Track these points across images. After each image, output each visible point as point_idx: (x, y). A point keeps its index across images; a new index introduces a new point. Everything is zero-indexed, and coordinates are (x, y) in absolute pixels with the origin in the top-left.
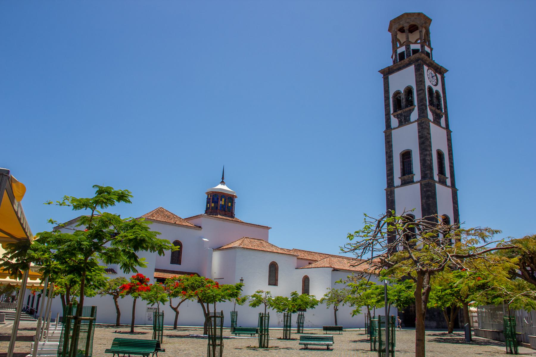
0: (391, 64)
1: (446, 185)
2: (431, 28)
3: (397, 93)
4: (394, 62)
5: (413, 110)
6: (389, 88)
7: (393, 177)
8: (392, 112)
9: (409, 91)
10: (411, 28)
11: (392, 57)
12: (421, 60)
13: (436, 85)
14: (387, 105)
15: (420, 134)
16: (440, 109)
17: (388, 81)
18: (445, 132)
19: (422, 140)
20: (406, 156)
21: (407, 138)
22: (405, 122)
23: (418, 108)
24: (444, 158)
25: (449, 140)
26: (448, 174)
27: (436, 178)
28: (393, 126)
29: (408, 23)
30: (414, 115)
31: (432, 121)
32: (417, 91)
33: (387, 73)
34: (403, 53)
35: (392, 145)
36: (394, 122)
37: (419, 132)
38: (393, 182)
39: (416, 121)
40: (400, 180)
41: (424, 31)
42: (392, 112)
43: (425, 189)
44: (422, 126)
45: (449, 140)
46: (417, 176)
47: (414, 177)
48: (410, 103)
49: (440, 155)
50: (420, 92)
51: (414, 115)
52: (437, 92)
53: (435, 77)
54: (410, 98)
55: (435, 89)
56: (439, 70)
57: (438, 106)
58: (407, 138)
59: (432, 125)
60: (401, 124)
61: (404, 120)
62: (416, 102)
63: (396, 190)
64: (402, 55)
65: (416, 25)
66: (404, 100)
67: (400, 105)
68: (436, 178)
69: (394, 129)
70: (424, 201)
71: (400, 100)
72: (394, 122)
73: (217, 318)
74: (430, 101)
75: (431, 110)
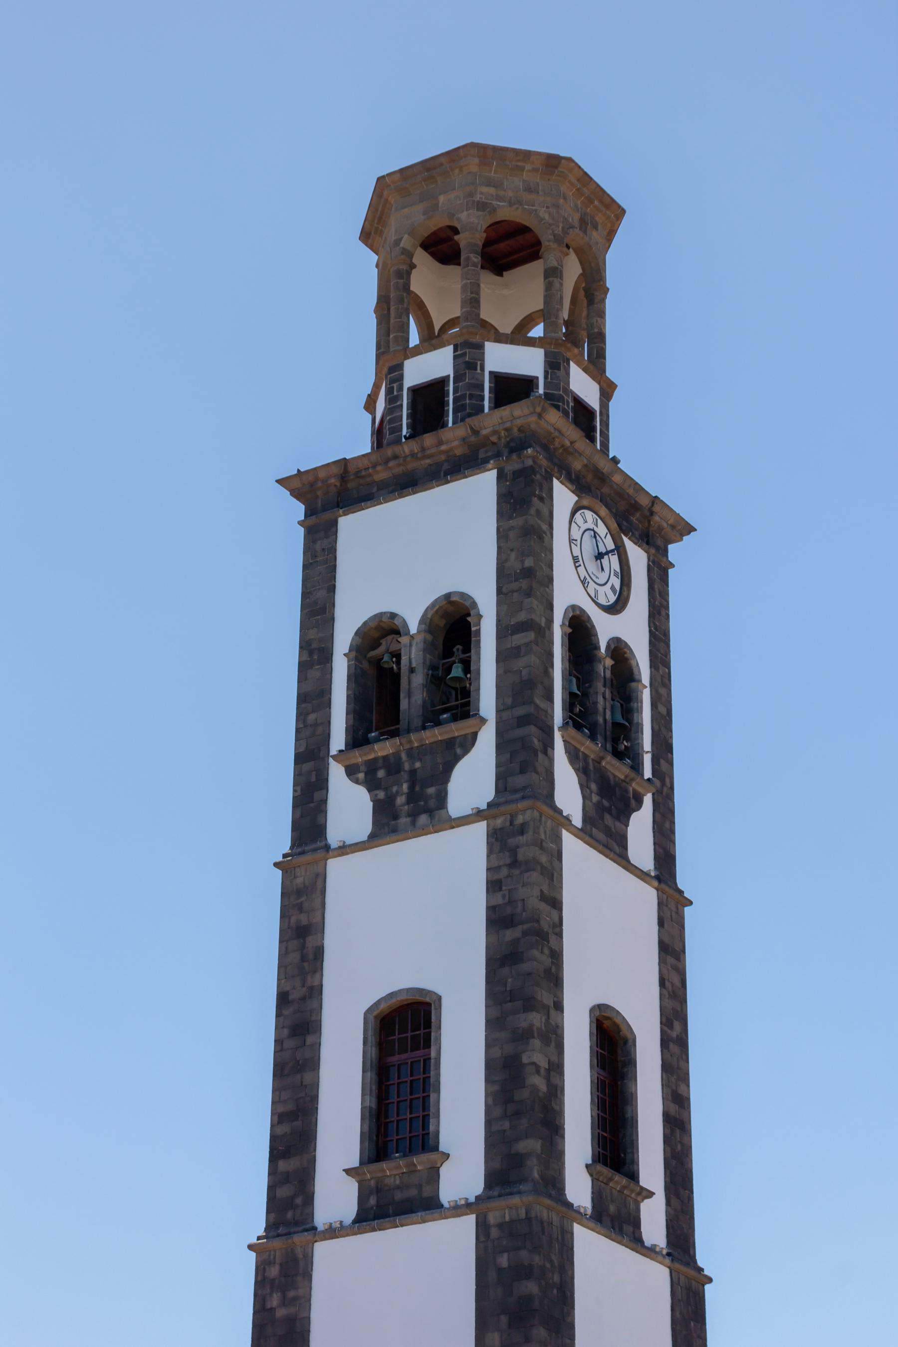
0: (357, 443)
1: (636, 1242)
2: (619, 263)
3: (382, 631)
4: (378, 434)
5: (468, 742)
6: (332, 589)
7: (313, 1161)
8: (338, 740)
9: (453, 625)
10: (493, 248)
11: (370, 405)
12: (536, 443)
13: (616, 608)
14: (312, 701)
15: (498, 899)
16: (632, 756)
17: (332, 551)
18: (647, 896)
19: (510, 935)
20: (404, 1030)
21: (413, 915)
22: (414, 815)
23: (499, 733)
24: (631, 1062)
25: (671, 951)
26: (651, 1168)
27: (579, 1188)
28: (335, 834)
29: (482, 206)
30: (473, 780)
31: (577, 821)
32: (503, 632)
33: (329, 497)
34: (439, 384)
35: (319, 953)
37: (493, 886)
38: (309, 1199)
39: (479, 815)
41: (572, 270)
42: (338, 740)
43: (504, 1261)
44: (514, 851)
45: (671, 951)
46: (463, 1170)
47: (446, 1172)
48: (454, 699)
49: (611, 1043)
50: (518, 639)
51: (473, 780)
52: (619, 651)
53: (614, 559)
54: (457, 671)
55: (606, 628)
56: (642, 522)
57: (620, 737)
58: (413, 915)
59: (570, 844)
60: (388, 824)
64: (429, 398)
65: (524, 230)
66: (419, 679)
67: (391, 708)
68: (579, 1188)
69: (345, 849)
71: (396, 677)
74: (571, 701)
75: (574, 756)
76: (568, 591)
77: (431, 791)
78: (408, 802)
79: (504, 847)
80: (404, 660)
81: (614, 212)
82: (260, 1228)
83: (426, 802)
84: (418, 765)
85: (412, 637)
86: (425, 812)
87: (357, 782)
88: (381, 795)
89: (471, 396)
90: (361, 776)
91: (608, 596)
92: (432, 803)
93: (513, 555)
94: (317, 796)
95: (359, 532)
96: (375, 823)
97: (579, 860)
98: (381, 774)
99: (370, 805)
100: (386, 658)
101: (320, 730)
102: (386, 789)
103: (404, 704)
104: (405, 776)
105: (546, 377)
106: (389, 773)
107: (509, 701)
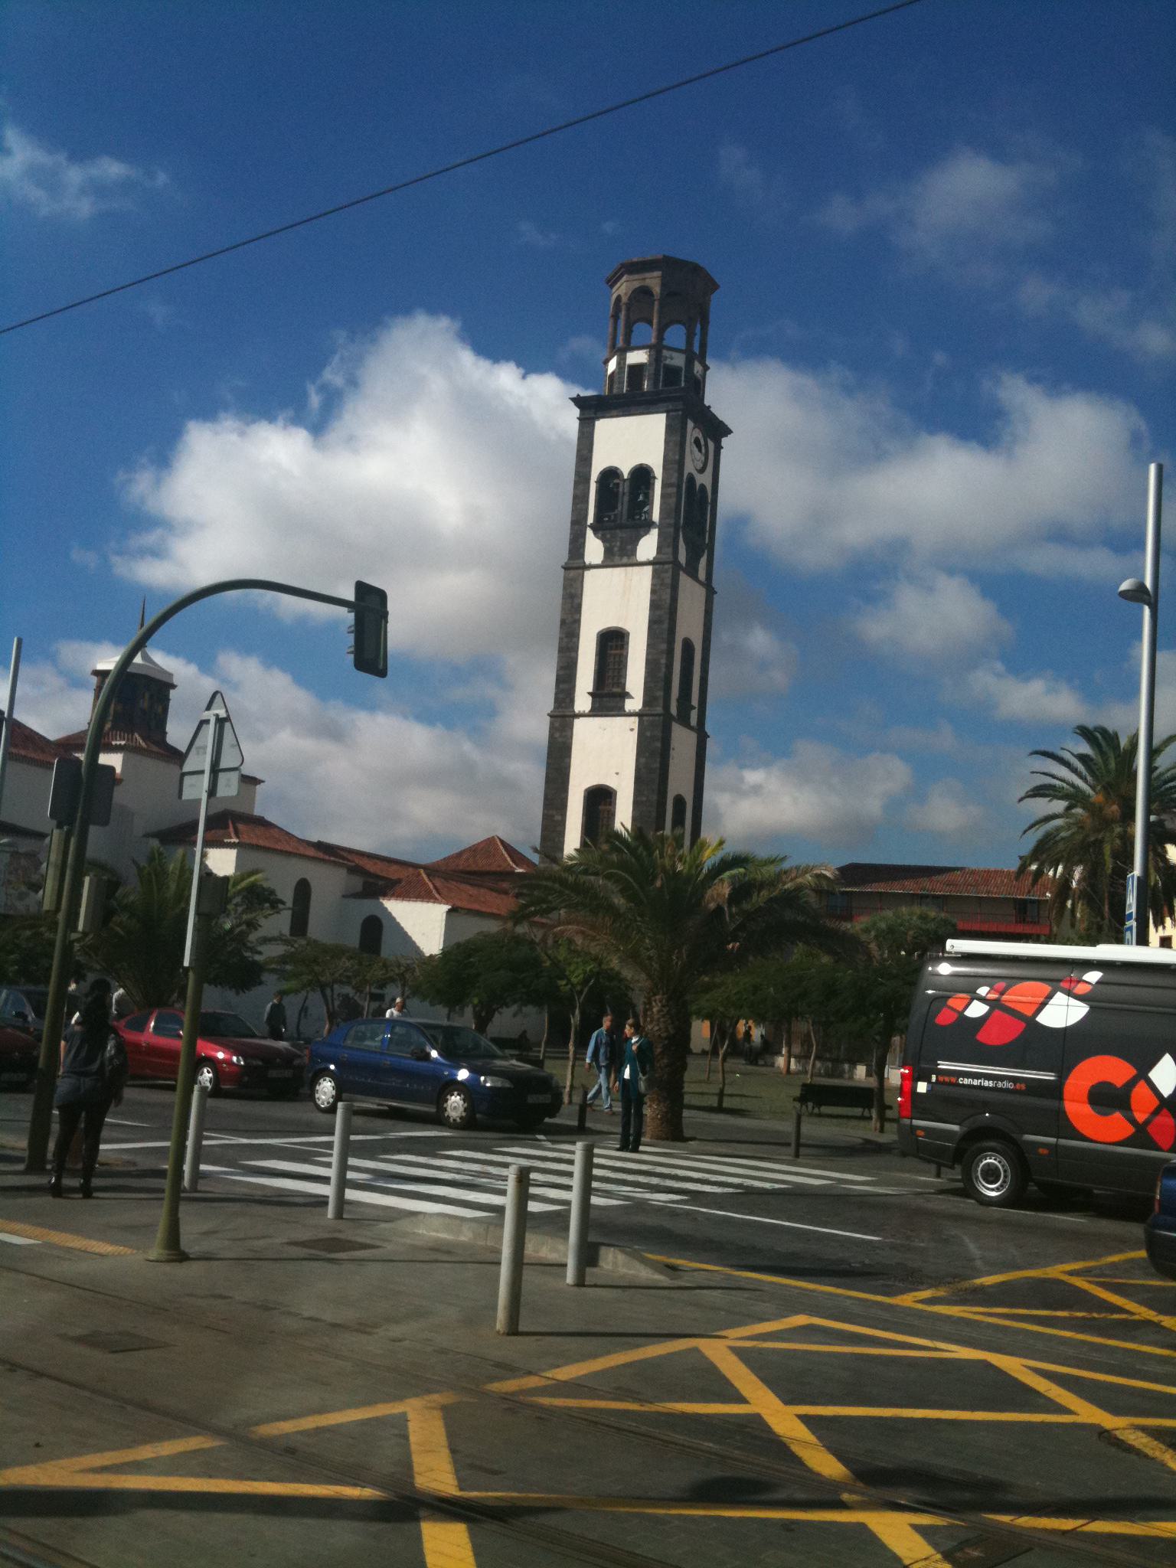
3: (610, 475)
8: (590, 520)
13: (702, 471)
14: (580, 499)
18: (701, 592)
19: (658, 613)
20: (613, 642)
22: (621, 556)
26: (695, 702)
27: (674, 711)
30: (648, 546)
32: (664, 486)
35: (580, 606)
36: (594, 549)
37: (653, 592)
40: (590, 698)
42: (590, 520)
43: (648, 734)
51: (648, 546)
52: (703, 486)
54: (641, 498)
56: (716, 430)
61: (619, 555)
62: (656, 516)
63: (578, 724)
64: (636, 370)
66: (626, 498)
68: (674, 711)
70: (643, 760)
72: (594, 549)
73: (725, 1105)
76: (689, 468)
81: (715, 287)
82: (552, 707)
91: (700, 465)
95: (605, 427)
97: (684, 579)
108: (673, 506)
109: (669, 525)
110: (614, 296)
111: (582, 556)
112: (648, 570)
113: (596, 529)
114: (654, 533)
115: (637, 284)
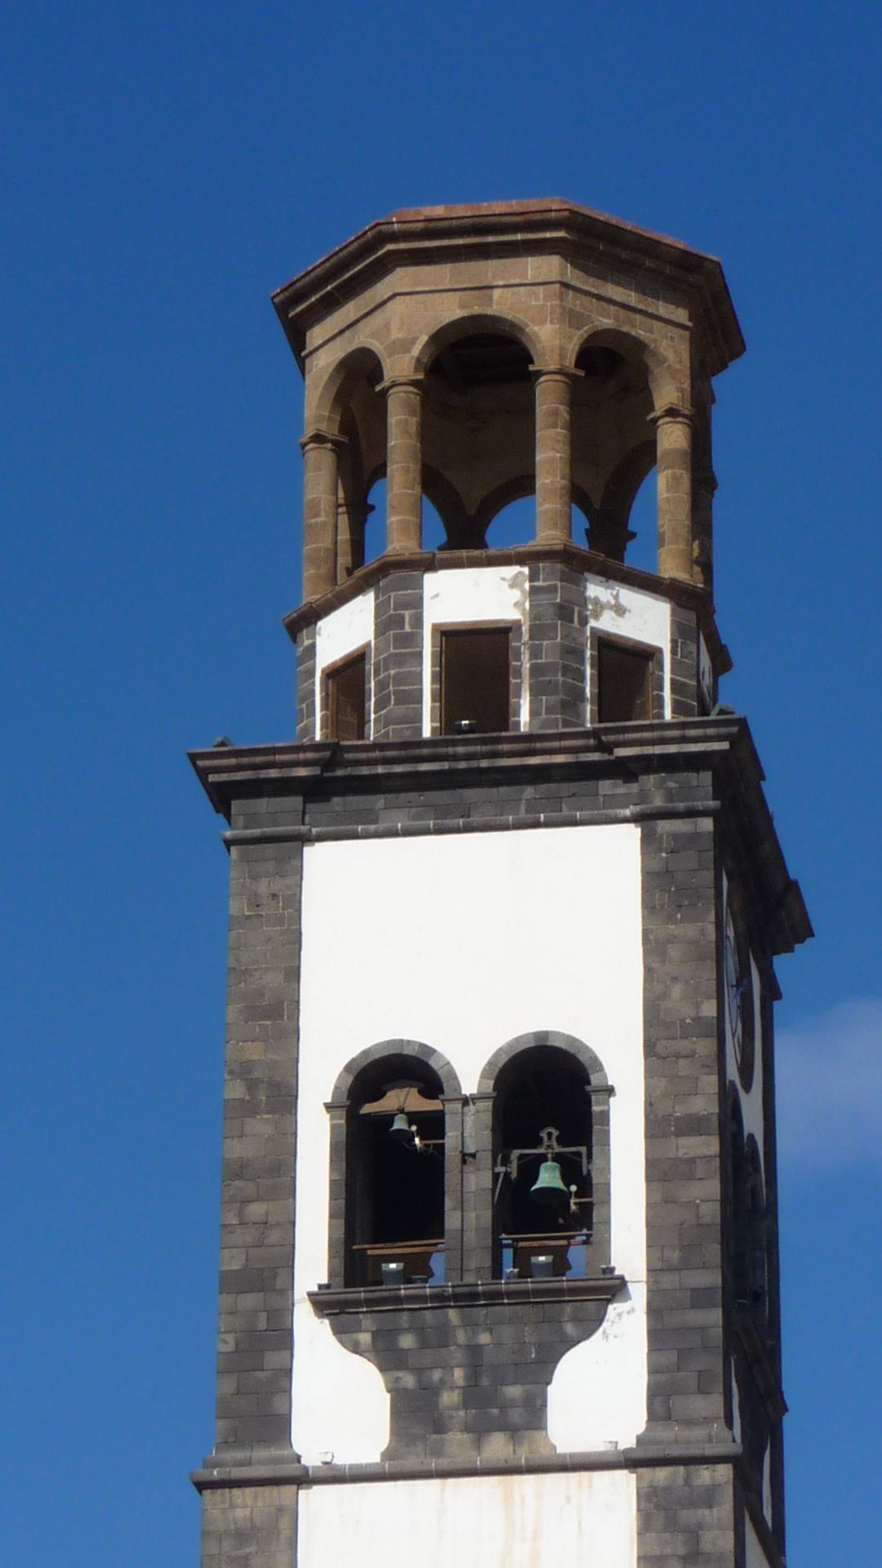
6: (294, 974)
8: (313, 1261)
9: (547, 1088)
22: (479, 1431)
32: (658, 1127)
36: (336, 1394)
51: (603, 1384)
54: (549, 1177)
62: (627, 1242)
72: (336, 1394)
77: (514, 1391)
78: (466, 1405)
79: (671, 1524)
80: (451, 1140)
83: (503, 1409)
84: (484, 1338)
85: (466, 1101)
86: (502, 1428)
87: (355, 1349)
88: (409, 1380)
89: (566, 670)
90: (365, 1338)
92: (516, 1415)
93: (677, 991)
94: (272, 1359)
96: (395, 1432)
98: (407, 1341)
99: (386, 1399)
100: (400, 1124)
101: (274, 1236)
102: (419, 1371)
103: (452, 1220)
104: (459, 1356)
105: (674, 652)
106: (424, 1344)
107: (675, 1256)
108: (711, 1211)
109: (698, 1299)
110: (324, 363)
111: (278, 1427)
112: (620, 1491)
113: (348, 1300)
114: (626, 1330)
115: (451, 310)
